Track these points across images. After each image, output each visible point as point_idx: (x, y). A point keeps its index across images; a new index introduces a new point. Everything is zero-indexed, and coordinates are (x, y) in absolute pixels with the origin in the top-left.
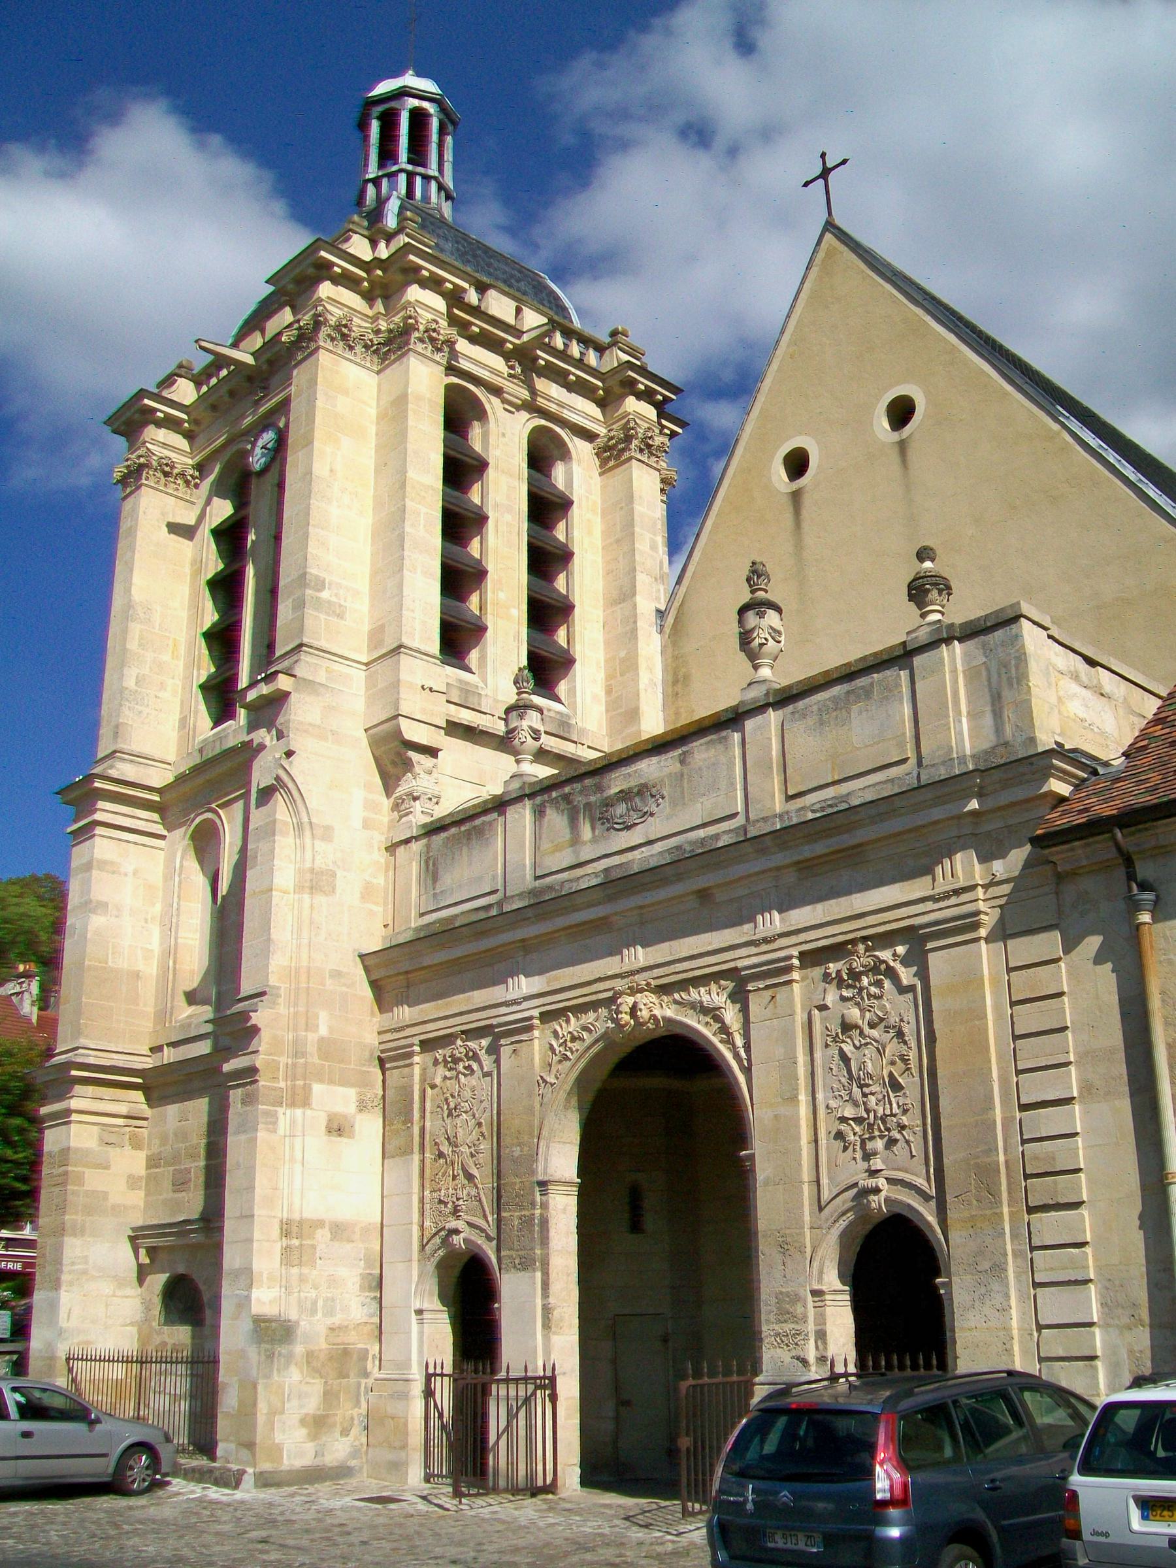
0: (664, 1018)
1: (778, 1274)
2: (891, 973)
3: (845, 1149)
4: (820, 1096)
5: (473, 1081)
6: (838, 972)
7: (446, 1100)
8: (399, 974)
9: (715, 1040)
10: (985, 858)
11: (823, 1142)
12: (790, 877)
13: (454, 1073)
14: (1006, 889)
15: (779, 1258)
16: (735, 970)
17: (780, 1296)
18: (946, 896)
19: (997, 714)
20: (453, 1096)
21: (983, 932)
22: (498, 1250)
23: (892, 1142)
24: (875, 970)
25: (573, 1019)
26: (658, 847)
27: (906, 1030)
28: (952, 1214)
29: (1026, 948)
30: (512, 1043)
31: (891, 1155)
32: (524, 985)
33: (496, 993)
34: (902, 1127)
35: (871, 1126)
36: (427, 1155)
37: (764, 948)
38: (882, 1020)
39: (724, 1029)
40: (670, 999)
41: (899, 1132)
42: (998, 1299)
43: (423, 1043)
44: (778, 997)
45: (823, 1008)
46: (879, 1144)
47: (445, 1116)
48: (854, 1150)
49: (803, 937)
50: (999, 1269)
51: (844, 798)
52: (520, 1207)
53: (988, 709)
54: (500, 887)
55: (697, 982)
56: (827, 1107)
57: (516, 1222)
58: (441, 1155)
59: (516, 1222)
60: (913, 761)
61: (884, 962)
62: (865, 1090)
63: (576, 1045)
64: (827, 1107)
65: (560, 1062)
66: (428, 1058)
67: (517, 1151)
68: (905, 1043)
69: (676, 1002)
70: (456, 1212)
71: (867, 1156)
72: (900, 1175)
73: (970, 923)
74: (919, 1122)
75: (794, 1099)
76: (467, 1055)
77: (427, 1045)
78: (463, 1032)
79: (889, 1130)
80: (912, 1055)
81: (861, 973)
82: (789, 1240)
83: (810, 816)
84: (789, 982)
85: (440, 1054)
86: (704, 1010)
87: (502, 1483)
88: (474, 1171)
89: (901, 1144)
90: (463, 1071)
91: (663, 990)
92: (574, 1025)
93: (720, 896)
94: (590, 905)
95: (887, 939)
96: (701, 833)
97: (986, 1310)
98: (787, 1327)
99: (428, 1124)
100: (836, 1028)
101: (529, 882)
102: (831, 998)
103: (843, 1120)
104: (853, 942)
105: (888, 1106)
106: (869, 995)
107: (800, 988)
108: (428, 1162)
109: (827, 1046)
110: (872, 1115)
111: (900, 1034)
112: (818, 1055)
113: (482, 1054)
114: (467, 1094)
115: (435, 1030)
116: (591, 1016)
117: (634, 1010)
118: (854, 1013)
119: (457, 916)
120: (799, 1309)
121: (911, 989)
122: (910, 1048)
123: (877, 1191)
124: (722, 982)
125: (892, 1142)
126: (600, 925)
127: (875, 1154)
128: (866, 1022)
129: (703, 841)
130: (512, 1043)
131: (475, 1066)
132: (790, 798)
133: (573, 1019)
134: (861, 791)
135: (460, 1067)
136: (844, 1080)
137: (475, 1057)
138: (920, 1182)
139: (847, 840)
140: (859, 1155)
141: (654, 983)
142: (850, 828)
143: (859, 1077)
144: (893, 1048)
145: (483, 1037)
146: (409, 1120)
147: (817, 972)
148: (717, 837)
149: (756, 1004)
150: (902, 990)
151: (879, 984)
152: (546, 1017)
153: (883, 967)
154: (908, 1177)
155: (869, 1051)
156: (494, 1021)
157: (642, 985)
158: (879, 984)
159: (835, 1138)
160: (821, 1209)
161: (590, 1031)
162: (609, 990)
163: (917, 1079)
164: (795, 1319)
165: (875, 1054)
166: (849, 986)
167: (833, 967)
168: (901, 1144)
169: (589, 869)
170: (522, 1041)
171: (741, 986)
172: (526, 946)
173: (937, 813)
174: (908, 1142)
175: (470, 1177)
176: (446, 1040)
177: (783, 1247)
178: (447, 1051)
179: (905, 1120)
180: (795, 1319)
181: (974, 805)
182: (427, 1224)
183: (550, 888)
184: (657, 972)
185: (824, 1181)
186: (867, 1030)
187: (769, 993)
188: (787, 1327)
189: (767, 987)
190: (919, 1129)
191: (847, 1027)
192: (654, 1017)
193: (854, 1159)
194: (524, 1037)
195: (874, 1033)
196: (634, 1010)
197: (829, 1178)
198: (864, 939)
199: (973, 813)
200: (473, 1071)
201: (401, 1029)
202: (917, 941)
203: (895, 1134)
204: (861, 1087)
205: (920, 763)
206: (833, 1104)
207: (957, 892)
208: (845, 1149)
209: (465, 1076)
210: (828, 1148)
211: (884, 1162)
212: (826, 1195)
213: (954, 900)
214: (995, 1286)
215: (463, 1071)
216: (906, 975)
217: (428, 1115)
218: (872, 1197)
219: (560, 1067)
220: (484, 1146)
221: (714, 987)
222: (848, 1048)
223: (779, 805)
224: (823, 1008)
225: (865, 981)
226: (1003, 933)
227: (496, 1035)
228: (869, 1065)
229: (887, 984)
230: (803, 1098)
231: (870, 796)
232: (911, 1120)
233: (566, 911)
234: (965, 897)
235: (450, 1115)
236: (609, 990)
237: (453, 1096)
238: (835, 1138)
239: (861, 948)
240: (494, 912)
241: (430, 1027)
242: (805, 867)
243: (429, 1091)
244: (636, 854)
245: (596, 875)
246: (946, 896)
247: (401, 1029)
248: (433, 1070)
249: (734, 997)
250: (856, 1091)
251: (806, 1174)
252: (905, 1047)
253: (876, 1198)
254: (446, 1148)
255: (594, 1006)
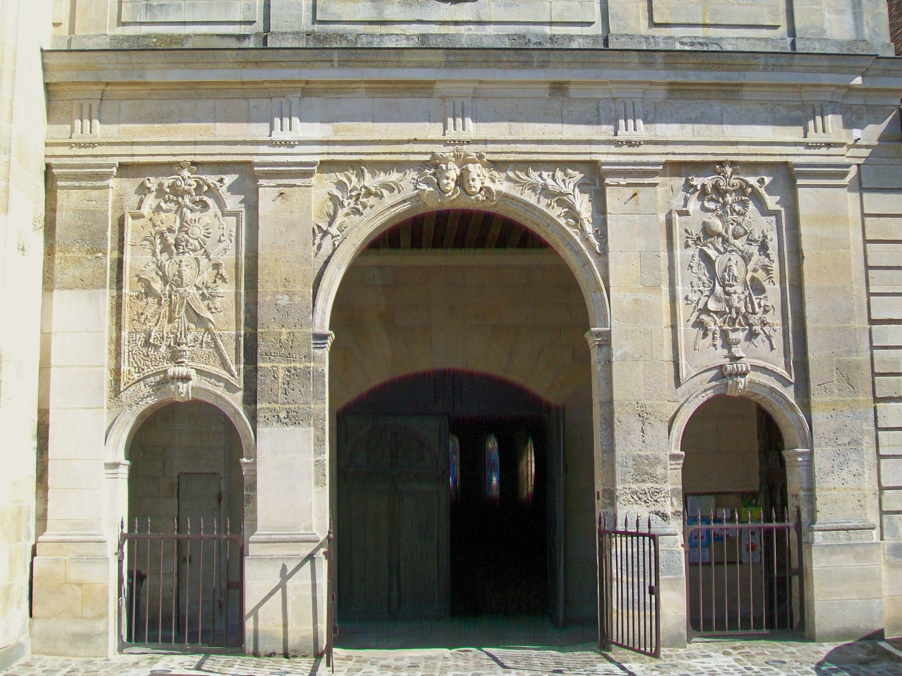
0: (499, 193)
1: (636, 437)
2: (756, 197)
3: (705, 335)
4: (680, 289)
5: (207, 218)
6: (704, 186)
7: (162, 234)
8: (96, 83)
9: (562, 221)
10: (848, 125)
11: (681, 328)
12: (660, 94)
13: (172, 206)
14: (866, 152)
15: (638, 426)
16: (594, 164)
17: (637, 460)
18: (818, 146)
19: (857, 16)
20: (170, 230)
21: (846, 181)
22: (251, 399)
23: (752, 335)
24: (741, 190)
25: (367, 175)
26: (491, 30)
27: (770, 244)
28: (816, 399)
29: (876, 202)
30: (279, 186)
31: (751, 346)
32: (301, 130)
33: (259, 131)
34: (764, 323)
35: (733, 321)
36: (126, 290)
37: (625, 149)
38: (746, 233)
39: (573, 214)
40: (503, 175)
41: (762, 329)
42: (854, 467)
43: (122, 166)
44: (640, 195)
45: (684, 213)
46: (741, 335)
47: (159, 248)
48: (714, 338)
49: (670, 149)
50: (855, 443)
51: (718, 41)
52: (288, 357)
53: (849, 10)
54: (259, 17)
55: (538, 165)
56: (686, 298)
57: (281, 374)
58: (149, 292)
59: (281, 374)
60: (783, 29)
61: (751, 186)
62: (727, 288)
63: (371, 200)
64: (686, 298)
65: (347, 214)
66: (129, 185)
67: (284, 300)
68: (768, 256)
69: (509, 179)
70: (175, 357)
71: (728, 344)
72: (762, 363)
73: (836, 172)
74: (779, 321)
75: (656, 287)
76: (199, 187)
77: (125, 169)
78: (193, 163)
79: (751, 325)
80: (775, 266)
81: (726, 191)
82: (648, 410)
83: (678, 47)
84: (655, 185)
85: (153, 183)
86: (545, 191)
87: (249, 646)
88: (207, 314)
89: (762, 336)
90: (190, 205)
91: (496, 165)
92: (370, 181)
93: (573, 91)
94: (422, 66)
95: (753, 167)
96: (548, 30)
97: (844, 474)
98: (646, 486)
99: (127, 258)
100: (696, 230)
101: (305, 23)
102: (694, 205)
103: (705, 310)
104: (721, 163)
105: (749, 305)
106: (733, 211)
107: (667, 192)
108: (126, 300)
109: (687, 246)
110: (733, 311)
111: (763, 248)
112: (678, 252)
113: (223, 190)
114: (198, 231)
115: (142, 155)
116: (394, 176)
117: (461, 181)
118: (717, 225)
119: (188, 36)
120: (659, 471)
121: (776, 214)
122: (773, 261)
123: (744, 374)
124: (570, 171)
125: (752, 335)
126: (423, 88)
127: (737, 343)
128: (730, 232)
129: (552, 38)
130: (279, 186)
131: (210, 202)
132: (653, 24)
133: (367, 175)
134: (732, 40)
135: (187, 200)
136: (704, 278)
137: (212, 191)
138: (781, 370)
139: (734, 77)
140: (719, 342)
141: (488, 157)
142: (747, 67)
143: (723, 278)
144: (757, 258)
145: (226, 173)
146: (97, 248)
147: (680, 181)
148: (571, 38)
149: (614, 198)
150: (764, 211)
151: (744, 204)
152: (327, 166)
153: (749, 190)
154: (769, 366)
155: (735, 257)
156: (256, 159)
157: (484, 156)
158: (744, 204)
159: (694, 326)
160: (678, 383)
161: (391, 190)
162: (427, 153)
163: (777, 286)
164: (653, 477)
165: (741, 262)
166: (711, 200)
167: (697, 182)
168: (762, 336)
169: (395, 29)
170: (294, 186)
171: (595, 178)
172: (307, 90)
173: (826, 79)
174: (769, 337)
175: (200, 321)
176: (170, 168)
177: (642, 417)
178: (167, 181)
179: (768, 318)
180: (653, 477)
181: (858, 81)
182: (125, 368)
183: (342, 36)
184: (491, 147)
185: (683, 362)
186: (732, 240)
187: (632, 190)
188: (646, 486)
189: (628, 185)
190: (779, 328)
191: (708, 232)
192: (488, 190)
193: (714, 345)
194: (298, 182)
195: (738, 243)
196: (461, 181)
197: (686, 359)
198: (732, 164)
199: (851, 89)
200: (205, 206)
201: (92, 145)
202: (787, 176)
203: (757, 328)
204: (723, 286)
205: (792, 32)
206: (694, 297)
207: (828, 145)
208: (705, 335)
209: (192, 211)
210: (685, 333)
211: (744, 351)
212: (683, 373)
213: (824, 151)
214: (853, 456)
215: (190, 205)
216: (772, 202)
217: (128, 249)
218: (739, 379)
219: (345, 219)
220: (226, 291)
221: (559, 174)
222: (712, 253)
223: (643, 27)
224: (684, 213)
225: (729, 199)
226: (861, 186)
227: (248, 176)
228: (734, 268)
229: (751, 205)
230: (665, 288)
231: (743, 47)
232: (774, 318)
233: (385, 64)
234: (833, 151)
235: (166, 248)
236: (427, 153)
237: (170, 230)
238: (694, 326)
239: (729, 170)
240: (251, 43)
241: (137, 150)
242: (676, 90)
243: (129, 222)
244: (462, 29)
245: (408, 38)
246: (818, 146)
247: (92, 145)
248: (137, 198)
249: (582, 186)
250: (718, 289)
251: (668, 354)
252: (767, 259)
253: (743, 380)
254: (158, 286)
255: (400, 166)
